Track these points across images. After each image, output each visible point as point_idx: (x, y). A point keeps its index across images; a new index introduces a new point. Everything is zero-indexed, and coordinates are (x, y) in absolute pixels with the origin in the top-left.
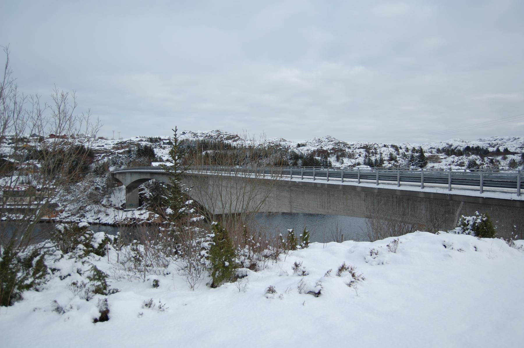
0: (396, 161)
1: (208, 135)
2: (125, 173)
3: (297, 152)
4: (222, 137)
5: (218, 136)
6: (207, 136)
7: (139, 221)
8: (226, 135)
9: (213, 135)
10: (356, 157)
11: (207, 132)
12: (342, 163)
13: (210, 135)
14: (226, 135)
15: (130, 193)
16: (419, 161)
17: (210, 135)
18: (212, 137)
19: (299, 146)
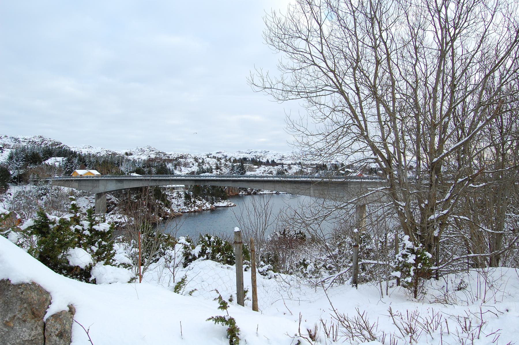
0: (221, 170)
1: (31, 140)
2: (98, 180)
3: (321, 163)
4: (46, 144)
5: (42, 142)
6: (30, 142)
7: (121, 224)
8: (50, 141)
9: (36, 140)
10: (207, 166)
11: (29, 138)
12: (181, 171)
13: (33, 141)
14: (50, 141)
15: (100, 199)
16: (240, 170)
17: (33, 141)
18: (35, 142)
19: (127, 154)
